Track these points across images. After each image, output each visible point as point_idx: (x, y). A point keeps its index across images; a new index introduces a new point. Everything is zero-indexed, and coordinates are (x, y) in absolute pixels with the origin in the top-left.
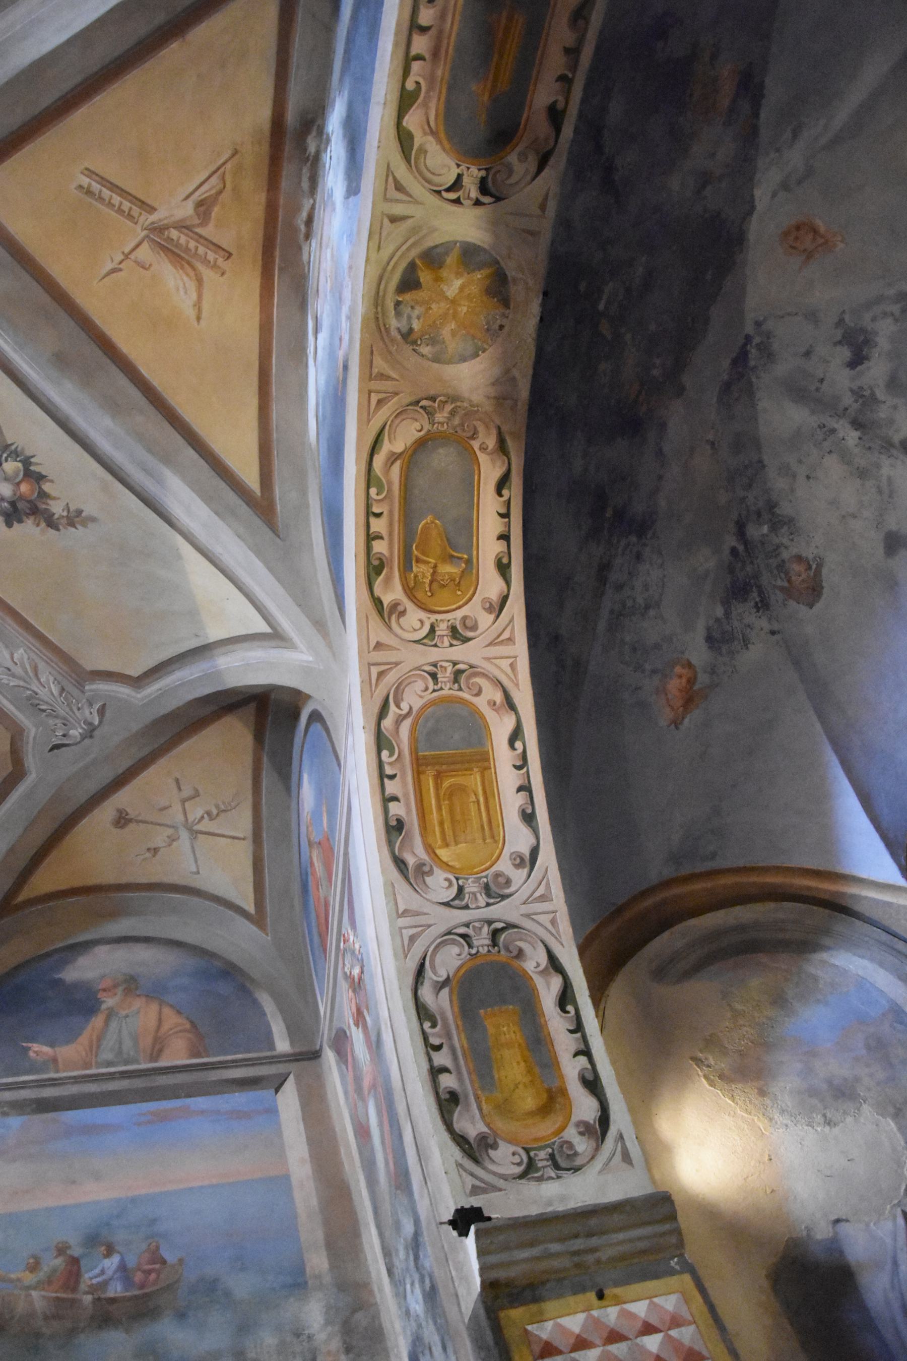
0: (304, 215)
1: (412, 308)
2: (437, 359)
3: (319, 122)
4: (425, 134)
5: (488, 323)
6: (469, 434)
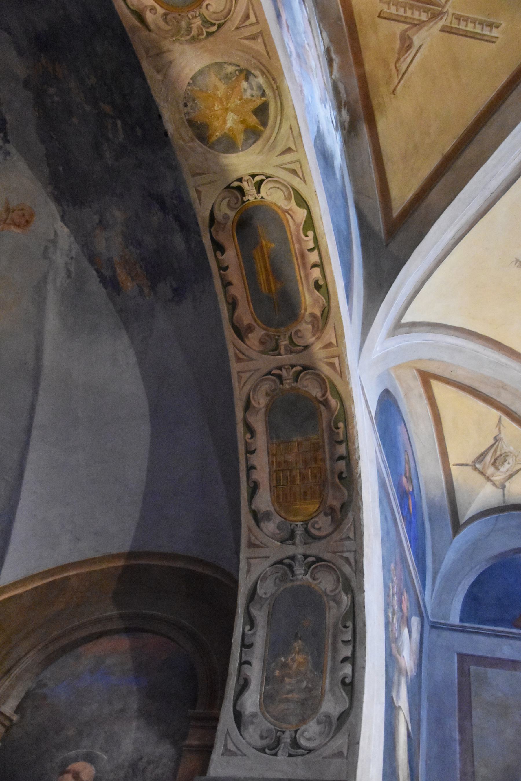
0: (335, 66)
1: (252, 96)
2: (220, 65)
3: (345, 132)
4: (291, 209)
5: (196, 104)
6: (169, 17)
